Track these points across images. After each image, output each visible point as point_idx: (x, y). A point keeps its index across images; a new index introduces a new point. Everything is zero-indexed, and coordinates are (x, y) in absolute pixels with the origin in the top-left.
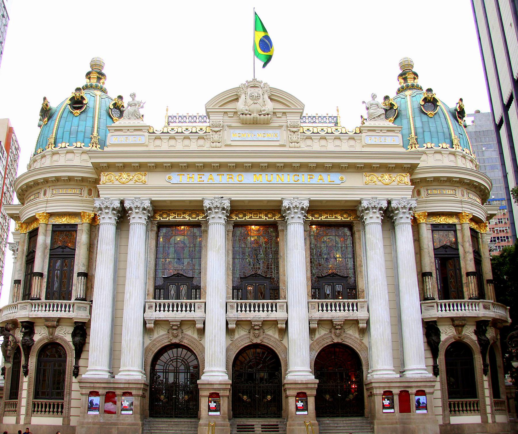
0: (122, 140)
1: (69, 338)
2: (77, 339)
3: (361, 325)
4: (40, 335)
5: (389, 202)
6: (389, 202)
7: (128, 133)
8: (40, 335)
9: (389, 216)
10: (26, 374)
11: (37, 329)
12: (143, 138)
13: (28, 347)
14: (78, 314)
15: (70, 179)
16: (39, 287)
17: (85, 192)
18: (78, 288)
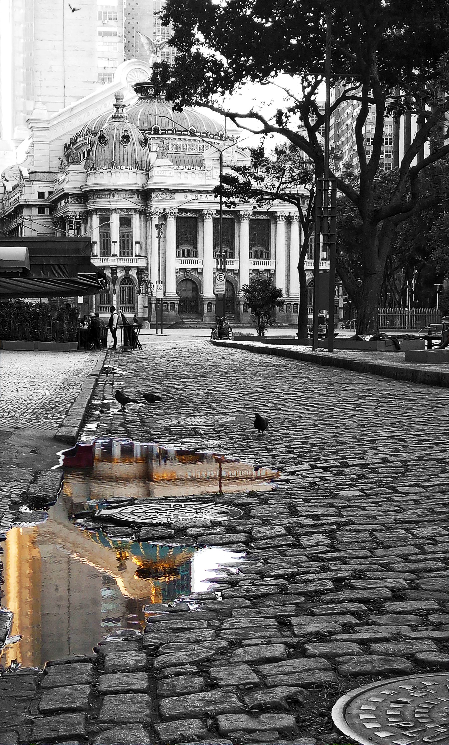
0: (161, 173)
1: (135, 275)
2: (140, 276)
3: (271, 272)
4: (120, 274)
5: (290, 213)
6: (290, 213)
7: (164, 169)
8: (120, 274)
9: (289, 220)
10: (115, 293)
11: (118, 271)
12: (172, 172)
13: (114, 280)
14: (142, 263)
15: (131, 190)
16: (116, 249)
17: (136, 197)
18: (136, 249)
